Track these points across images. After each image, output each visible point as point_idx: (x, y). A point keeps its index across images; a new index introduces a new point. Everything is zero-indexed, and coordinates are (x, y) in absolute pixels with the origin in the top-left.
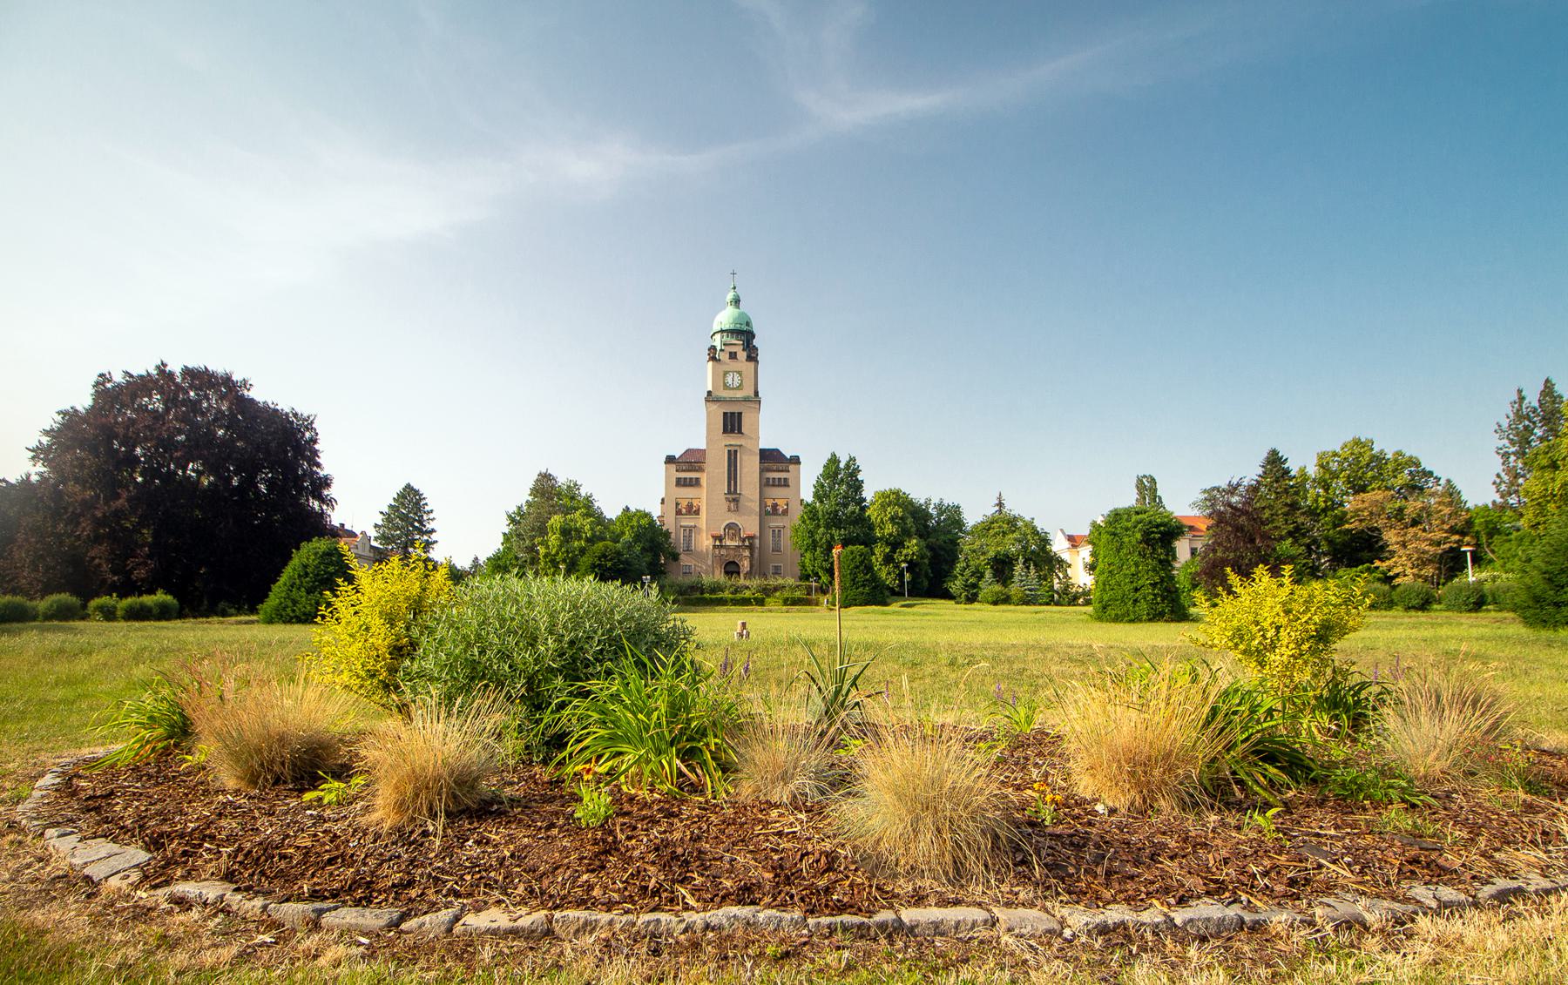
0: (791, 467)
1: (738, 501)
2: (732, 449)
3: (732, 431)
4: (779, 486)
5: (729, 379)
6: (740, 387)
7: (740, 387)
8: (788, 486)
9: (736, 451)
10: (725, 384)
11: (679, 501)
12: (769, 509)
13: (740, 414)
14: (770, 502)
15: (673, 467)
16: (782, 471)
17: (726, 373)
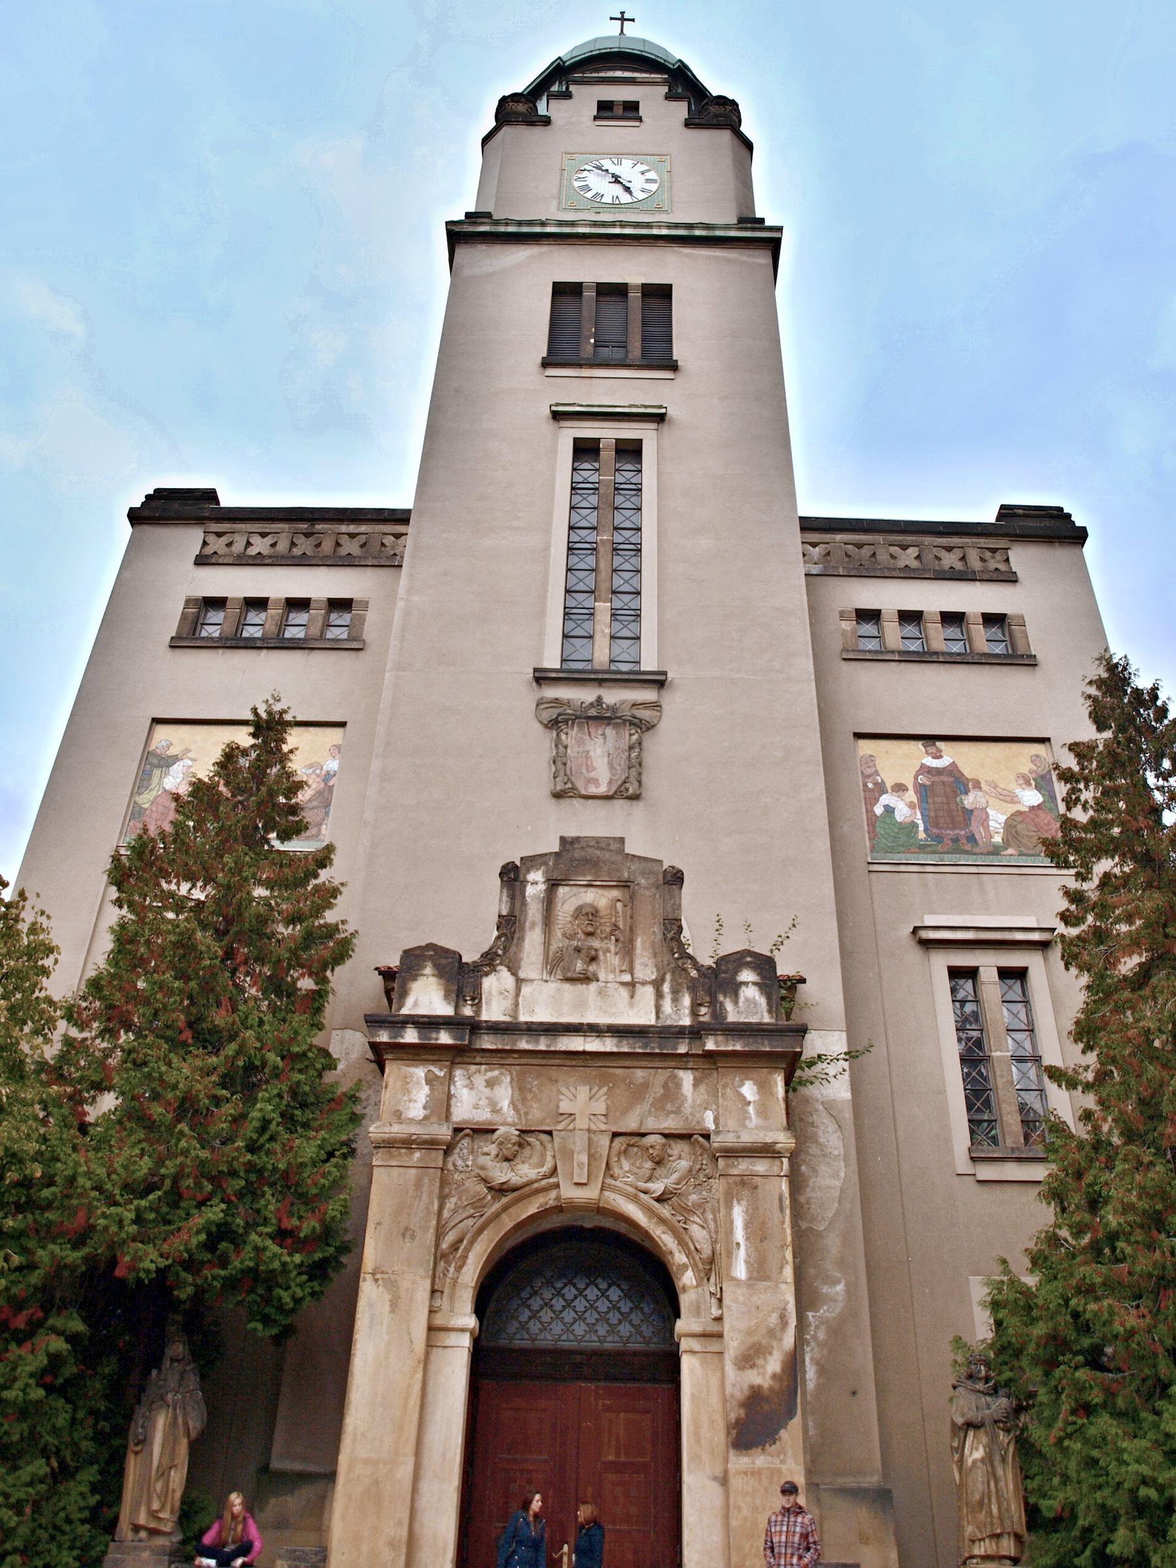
1: (644, 727)
8: (1029, 662)
12: (904, 809)
13: (660, 294)
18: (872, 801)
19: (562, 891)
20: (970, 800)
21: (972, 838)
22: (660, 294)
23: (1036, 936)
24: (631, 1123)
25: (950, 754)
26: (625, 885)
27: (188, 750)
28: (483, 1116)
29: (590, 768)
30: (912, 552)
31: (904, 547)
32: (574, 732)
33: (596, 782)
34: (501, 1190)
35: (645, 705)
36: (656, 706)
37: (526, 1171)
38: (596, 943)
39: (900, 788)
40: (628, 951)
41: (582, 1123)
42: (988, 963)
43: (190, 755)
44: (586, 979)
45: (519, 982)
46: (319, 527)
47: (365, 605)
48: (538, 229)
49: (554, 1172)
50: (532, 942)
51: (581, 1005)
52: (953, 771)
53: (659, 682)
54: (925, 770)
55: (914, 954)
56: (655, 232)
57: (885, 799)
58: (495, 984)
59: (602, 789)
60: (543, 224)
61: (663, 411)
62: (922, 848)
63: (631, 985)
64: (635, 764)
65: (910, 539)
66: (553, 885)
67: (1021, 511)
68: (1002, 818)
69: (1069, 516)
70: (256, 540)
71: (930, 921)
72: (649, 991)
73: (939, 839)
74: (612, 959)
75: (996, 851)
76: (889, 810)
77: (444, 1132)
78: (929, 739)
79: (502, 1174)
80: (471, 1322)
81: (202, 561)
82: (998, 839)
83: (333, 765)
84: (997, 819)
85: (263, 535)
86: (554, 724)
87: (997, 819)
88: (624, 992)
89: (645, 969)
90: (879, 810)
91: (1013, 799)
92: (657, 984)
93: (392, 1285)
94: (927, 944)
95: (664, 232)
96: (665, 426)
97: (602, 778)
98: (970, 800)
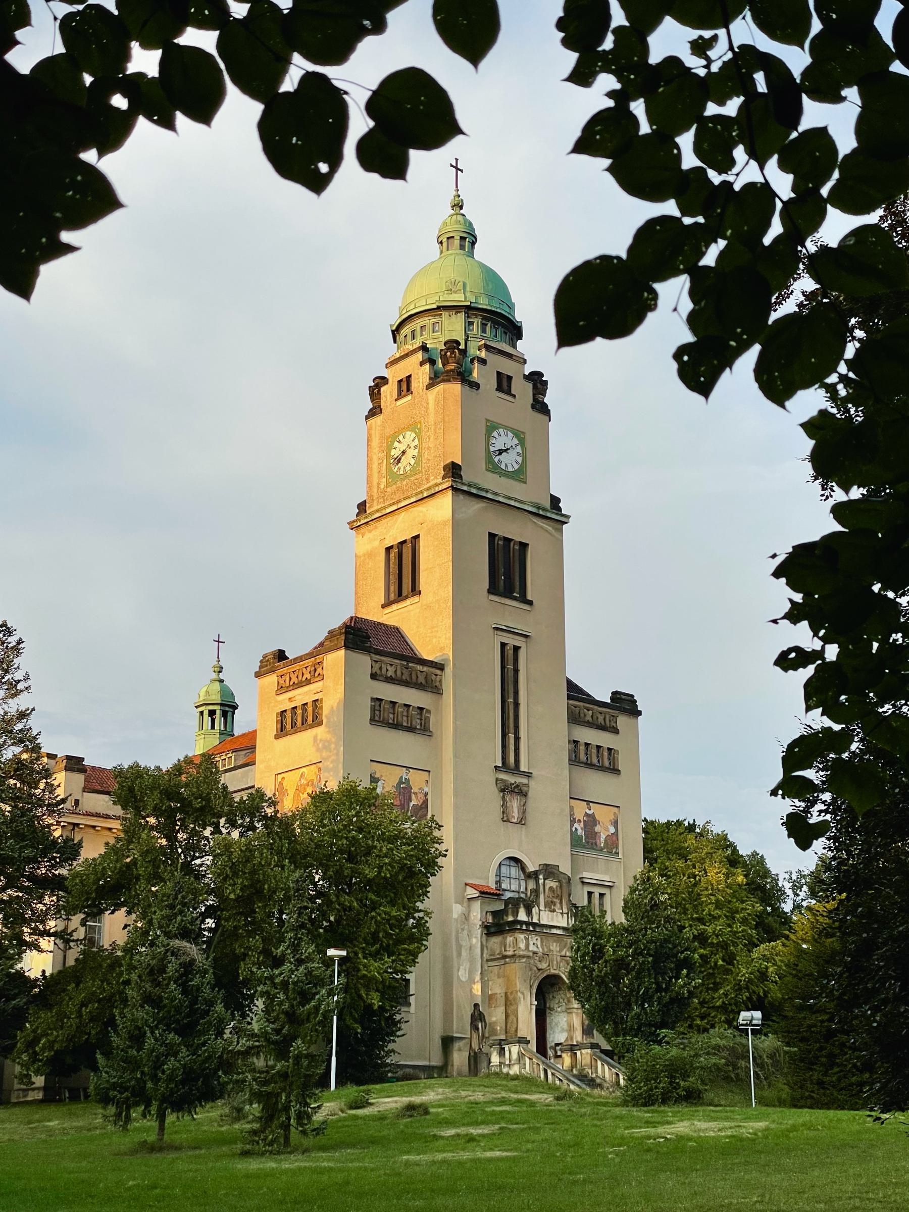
0: (622, 721)
2: (511, 641)
3: (507, 593)
4: (601, 768)
5: (502, 440)
6: (519, 475)
7: (519, 475)
9: (516, 649)
10: (489, 460)
11: (379, 770)
13: (524, 546)
14: (581, 810)
15: (364, 661)
16: (603, 728)
17: (491, 428)
18: (572, 826)
19: (546, 881)
20: (597, 829)
21: (596, 844)
22: (524, 546)
23: (610, 884)
24: (563, 953)
25: (595, 809)
26: (560, 881)
27: (382, 776)
28: (535, 949)
29: (513, 812)
30: (590, 712)
31: (588, 710)
32: (509, 796)
33: (513, 817)
34: (539, 970)
35: (524, 785)
36: (528, 786)
37: (544, 965)
38: (555, 900)
39: (579, 821)
40: (561, 903)
41: (555, 953)
42: (597, 891)
43: (383, 778)
44: (554, 911)
45: (540, 910)
46: (410, 665)
47: (429, 711)
48: (484, 494)
49: (549, 965)
50: (542, 896)
51: (552, 920)
52: (593, 816)
53: (528, 775)
54: (587, 815)
55: (580, 885)
56: (526, 507)
57: (576, 825)
58: (535, 910)
59: (515, 821)
60: (487, 491)
61: (530, 634)
62: (584, 847)
63: (562, 913)
64: (523, 813)
65: (591, 706)
66: (545, 879)
67: (623, 697)
68: (604, 837)
69: (636, 701)
70: (389, 668)
71: (585, 875)
72: (565, 915)
73: (588, 843)
74: (558, 905)
75: (601, 850)
76: (576, 829)
77: (531, 954)
78: (588, 802)
79: (540, 967)
80: (536, 1003)
81: (374, 676)
82: (602, 845)
83: (426, 789)
84: (603, 837)
85: (391, 665)
86: (502, 791)
87: (603, 837)
88: (560, 916)
89: (565, 910)
90: (574, 830)
91: (607, 830)
92: (567, 914)
93: (523, 994)
94: (583, 883)
95: (530, 509)
96: (528, 640)
97: (515, 815)
98: (597, 829)
